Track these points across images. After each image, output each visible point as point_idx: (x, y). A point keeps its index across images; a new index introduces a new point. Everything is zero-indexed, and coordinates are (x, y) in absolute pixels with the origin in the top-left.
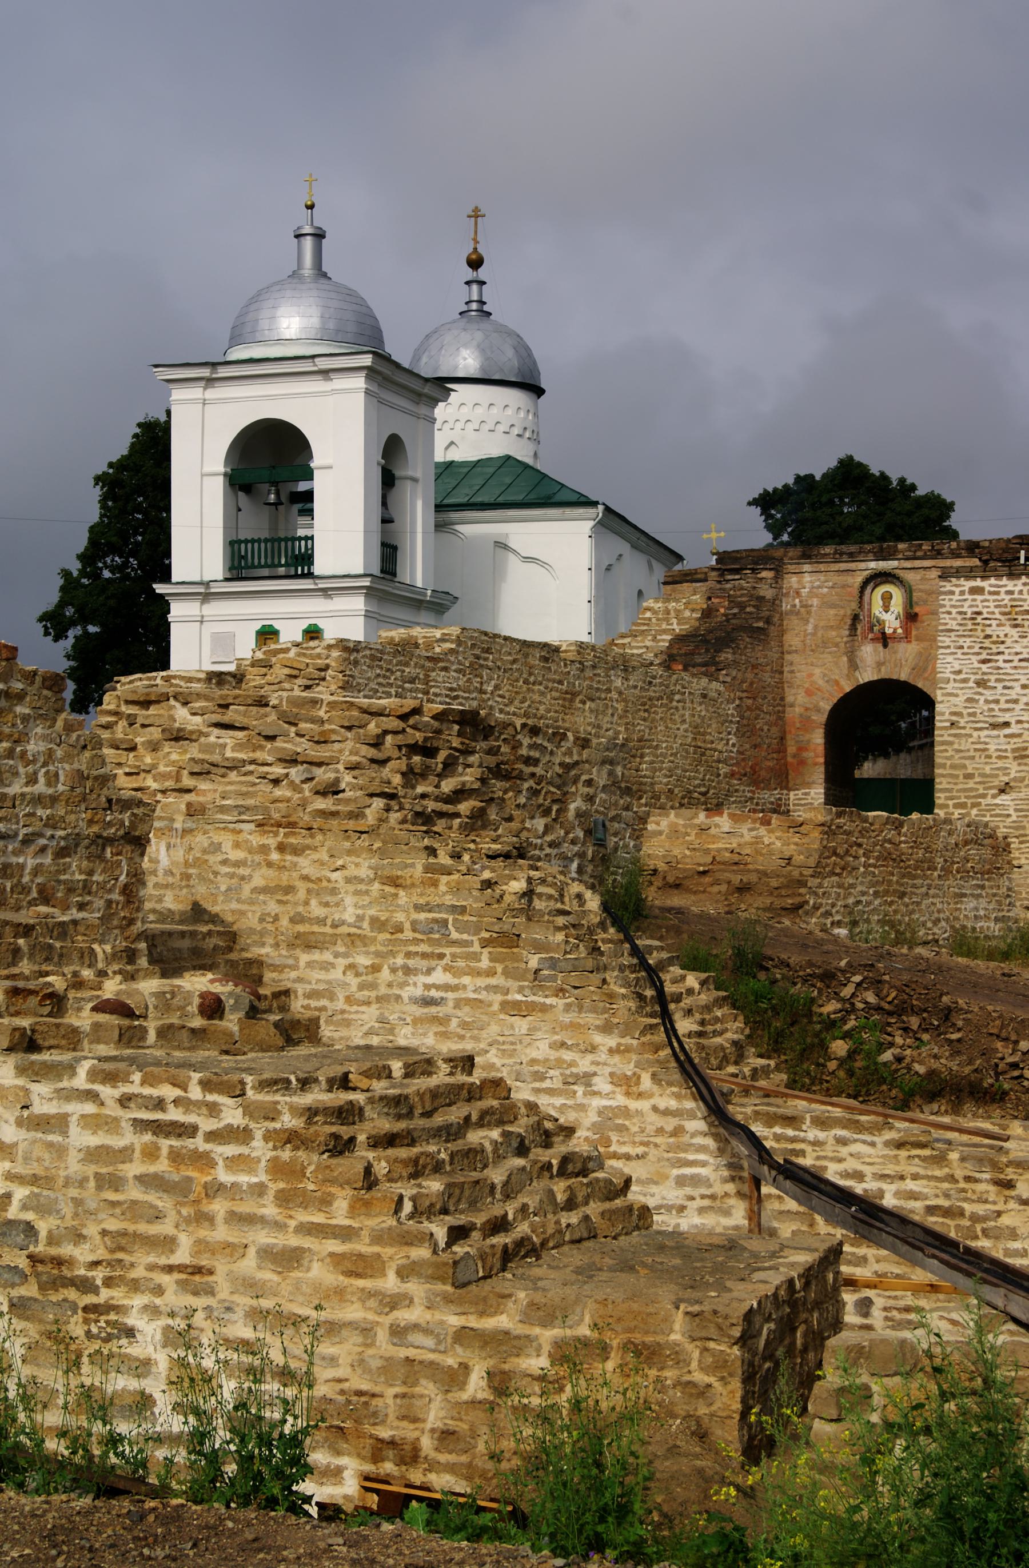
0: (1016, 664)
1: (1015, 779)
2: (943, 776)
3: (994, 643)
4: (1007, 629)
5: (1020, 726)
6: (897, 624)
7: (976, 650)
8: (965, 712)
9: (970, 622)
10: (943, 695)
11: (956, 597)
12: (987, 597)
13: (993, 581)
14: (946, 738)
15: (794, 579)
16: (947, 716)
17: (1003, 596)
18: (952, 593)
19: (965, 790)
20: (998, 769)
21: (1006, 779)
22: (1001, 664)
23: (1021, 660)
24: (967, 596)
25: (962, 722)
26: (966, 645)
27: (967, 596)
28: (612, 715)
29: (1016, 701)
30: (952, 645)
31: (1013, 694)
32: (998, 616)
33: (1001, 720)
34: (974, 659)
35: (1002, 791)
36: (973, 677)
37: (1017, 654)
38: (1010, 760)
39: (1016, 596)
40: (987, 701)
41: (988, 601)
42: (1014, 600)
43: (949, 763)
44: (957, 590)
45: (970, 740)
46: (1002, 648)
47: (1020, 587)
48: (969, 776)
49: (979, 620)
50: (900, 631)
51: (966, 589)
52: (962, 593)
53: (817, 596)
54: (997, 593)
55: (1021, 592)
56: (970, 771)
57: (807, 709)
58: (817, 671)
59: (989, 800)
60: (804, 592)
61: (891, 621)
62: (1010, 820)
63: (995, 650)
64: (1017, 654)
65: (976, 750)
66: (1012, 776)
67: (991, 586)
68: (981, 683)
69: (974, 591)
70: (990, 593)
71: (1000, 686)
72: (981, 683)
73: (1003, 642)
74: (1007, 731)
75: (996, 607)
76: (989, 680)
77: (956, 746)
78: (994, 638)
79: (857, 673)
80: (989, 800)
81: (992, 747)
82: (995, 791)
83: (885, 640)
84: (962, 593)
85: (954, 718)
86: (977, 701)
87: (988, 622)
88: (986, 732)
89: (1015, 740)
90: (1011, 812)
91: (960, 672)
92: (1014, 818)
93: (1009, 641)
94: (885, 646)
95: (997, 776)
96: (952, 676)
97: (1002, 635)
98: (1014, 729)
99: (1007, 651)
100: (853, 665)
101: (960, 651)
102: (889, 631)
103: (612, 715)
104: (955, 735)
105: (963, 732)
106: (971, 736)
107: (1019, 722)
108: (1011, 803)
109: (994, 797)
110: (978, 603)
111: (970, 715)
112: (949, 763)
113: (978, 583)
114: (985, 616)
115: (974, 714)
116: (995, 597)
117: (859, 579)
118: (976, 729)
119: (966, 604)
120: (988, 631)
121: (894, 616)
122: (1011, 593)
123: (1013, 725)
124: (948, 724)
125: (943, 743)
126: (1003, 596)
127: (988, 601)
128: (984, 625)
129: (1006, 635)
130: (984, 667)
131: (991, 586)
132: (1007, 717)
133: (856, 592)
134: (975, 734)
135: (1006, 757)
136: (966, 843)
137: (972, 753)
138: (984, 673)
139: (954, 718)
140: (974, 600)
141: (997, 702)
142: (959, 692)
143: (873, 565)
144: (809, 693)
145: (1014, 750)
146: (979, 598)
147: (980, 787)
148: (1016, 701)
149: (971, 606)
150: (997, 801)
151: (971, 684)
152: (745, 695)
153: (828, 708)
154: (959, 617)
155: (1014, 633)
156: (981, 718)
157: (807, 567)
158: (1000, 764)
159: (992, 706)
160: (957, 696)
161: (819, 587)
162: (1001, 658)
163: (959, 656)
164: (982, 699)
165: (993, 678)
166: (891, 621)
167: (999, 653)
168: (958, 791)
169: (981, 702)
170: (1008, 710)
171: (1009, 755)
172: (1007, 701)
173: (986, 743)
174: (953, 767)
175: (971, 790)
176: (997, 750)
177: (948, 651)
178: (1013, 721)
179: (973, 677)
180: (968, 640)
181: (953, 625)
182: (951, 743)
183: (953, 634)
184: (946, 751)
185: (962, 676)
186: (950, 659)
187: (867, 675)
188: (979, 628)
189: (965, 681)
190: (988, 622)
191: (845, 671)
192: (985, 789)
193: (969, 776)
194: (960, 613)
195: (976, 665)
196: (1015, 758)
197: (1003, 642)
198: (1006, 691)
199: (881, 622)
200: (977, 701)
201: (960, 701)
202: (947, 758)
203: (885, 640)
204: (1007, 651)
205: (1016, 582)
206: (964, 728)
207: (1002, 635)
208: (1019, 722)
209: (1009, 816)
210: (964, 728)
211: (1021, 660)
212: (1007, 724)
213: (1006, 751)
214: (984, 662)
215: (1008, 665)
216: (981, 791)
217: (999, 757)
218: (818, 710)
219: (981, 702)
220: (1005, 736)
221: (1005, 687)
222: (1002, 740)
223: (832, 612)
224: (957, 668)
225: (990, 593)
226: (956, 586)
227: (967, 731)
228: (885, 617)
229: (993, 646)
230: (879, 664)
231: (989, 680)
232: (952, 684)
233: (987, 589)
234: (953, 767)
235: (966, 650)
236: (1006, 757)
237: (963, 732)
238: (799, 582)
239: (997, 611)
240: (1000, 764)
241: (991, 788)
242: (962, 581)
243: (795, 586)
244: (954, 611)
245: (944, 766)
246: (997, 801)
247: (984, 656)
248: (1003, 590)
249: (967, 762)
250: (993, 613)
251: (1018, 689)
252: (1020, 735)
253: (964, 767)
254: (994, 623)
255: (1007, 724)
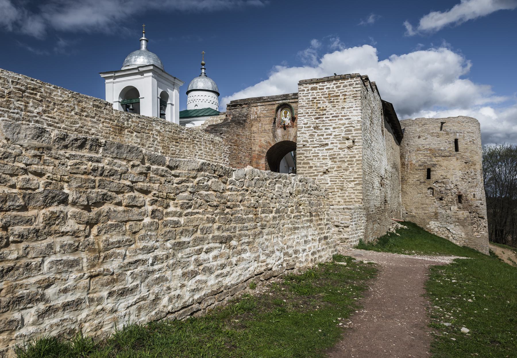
0: (331, 118)
1: (330, 168)
2: (300, 167)
3: (322, 110)
4: (327, 104)
5: (332, 145)
6: (289, 122)
7: (314, 114)
8: (309, 140)
9: (311, 102)
10: (301, 134)
11: (305, 92)
12: (319, 91)
13: (321, 84)
14: (301, 152)
15: (255, 108)
16: (301, 142)
17: (325, 90)
18: (304, 90)
19: (309, 173)
20: (323, 164)
21: (326, 168)
22: (324, 119)
23: (333, 117)
24: (310, 91)
25: (308, 145)
26: (309, 112)
27: (310, 91)
28: (154, 141)
29: (331, 135)
30: (304, 112)
31: (329, 132)
32: (323, 99)
33: (324, 143)
34: (313, 117)
35: (325, 173)
36: (312, 125)
37: (331, 114)
38: (328, 160)
39: (331, 89)
40: (318, 135)
41: (319, 92)
42: (330, 91)
43: (302, 162)
44: (306, 89)
45: (311, 152)
46: (325, 112)
47: (331, 86)
48: (311, 167)
49: (315, 101)
50: (290, 124)
51: (310, 88)
52: (308, 90)
53: (262, 114)
54: (323, 89)
55: (333, 88)
56: (311, 165)
57: (259, 152)
58: (263, 139)
59: (319, 177)
60: (258, 113)
61: (287, 121)
62: (328, 185)
63: (322, 113)
64: (331, 114)
65: (314, 156)
66: (329, 167)
67: (320, 86)
68: (316, 128)
69: (313, 89)
70: (320, 89)
71: (324, 128)
72: (316, 128)
73: (325, 110)
74: (327, 147)
75: (322, 95)
76: (319, 126)
77: (305, 155)
78: (322, 108)
79: (276, 139)
80: (319, 177)
81: (320, 155)
82: (321, 173)
83: (285, 127)
84: (308, 90)
85: (305, 143)
86: (314, 135)
87: (319, 102)
88: (318, 148)
89: (330, 151)
90: (329, 182)
91: (307, 123)
92: (330, 184)
93: (327, 109)
94: (285, 129)
95: (322, 167)
96: (304, 126)
97: (325, 107)
98: (330, 146)
99: (327, 113)
100: (275, 136)
101: (307, 115)
102: (286, 124)
103: (154, 141)
104: (305, 150)
105: (308, 148)
106: (311, 150)
107: (332, 143)
108: (329, 178)
109: (321, 176)
110: (315, 94)
111: (311, 141)
112: (302, 162)
113: (315, 85)
114: (318, 99)
115: (313, 141)
116: (322, 91)
117: (275, 107)
118: (314, 147)
119: (310, 95)
120: (319, 105)
121: (288, 119)
122: (329, 88)
123: (329, 145)
124: (302, 146)
125: (300, 154)
126: (325, 90)
127: (319, 92)
128: (317, 103)
129: (326, 107)
130: (317, 121)
131: (320, 86)
132: (327, 142)
133: (275, 110)
134: (313, 149)
135: (327, 159)
136: (299, 192)
137: (312, 158)
138: (317, 124)
139: (305, 143)
140: (313, 93)
141: (323, 135)
142: (307, 132)
143: (281, 102)
144: (260, 146)
145: (330, 156)
146: (315, 91)
147: (315, 172)
148: (331, 135)
149: (312, 95)
150: (322, 177)
151: (311, 128)
152: (233, 144)
153: (266, 151)
154: (307, 101)
155: (330, 105)
156: (316, 143)
157: (259, 104)
158: (324, 162)
159: (321, 137)
160: (306, 134)
161: (263, 111)
162: (324, 116)
163: (307, 117)
164: (316, 134)
165: (321, 125)
166: (287, 121)
167: (323, 115)
168: (306, 174)
169: (316, 136)
170: (327, 138)
171: (327, 157)
172: (327, 135)
173: (318, 153)
174: (304, 163)
175: (312, 173)
176: (322, 156)
177: (302, 115)
178: (329, 143)
179: (312, 125)
180: (310, 110)
181: (304, 104)
182: (303, 154)
183: (304, 108)
184: (301, 157)
185: (308, 125)
186: (303, 118)
187: (279, 139)
188: (315, 104)
189: (309, 127)
190: (319, 102)
191: (272, 139)
192: (317, 173)
193: (311, 167)
194: (307, 99)
195: (314, 120)
196: (331, 159)
197: (325, 110)
198: (326, 131)
199: (284, 121)
200: (314, 135)
201: (307, 136)
202: (301, 160)
203: (285, 127)
204: (327, 113)
205: (331, 83)
206: (309, 147)
207: (325, 107)
208: (332, 143)
209: (327, 183)
210: (309, 147)
211: (333, 117)
212: (327, 144)
213: (326, 156)
214: (317, 118)
215: (327, 119)
216: (316, 174)
217: (323, 159)
218: (263, 152)
219: (316, 136)
220: (326, 150)
221: (326, 129)
222: (325, 151)
223: (268, 119)
224: (306, 122)
225: (320, 89)
226: (306, 87)
227: (310, 148)
228: (285, 119)
229: (321, 112)
230: (283, 136)
231: (319, 126)
232: (304, 129)
233: (319, 87)
234: (304, 163)
235: (309, 114)
236: (327, 159)
237: (308, 148)
238: (257, 109)
239: (322, 96)
240: (324, 162)
241: (320, 172)
242: (308, 85)
243: (256, 111)
244: (304, 98)
245: (300, 163)
246: (322, 177)
247: (317, 116)
248: (325, 87)
249: (310, 161)
250: (321, 98)
251: (332, 130)
252: (332, 149)
253: (309, 163)
254: (321, 102)
255: (327, 144)
